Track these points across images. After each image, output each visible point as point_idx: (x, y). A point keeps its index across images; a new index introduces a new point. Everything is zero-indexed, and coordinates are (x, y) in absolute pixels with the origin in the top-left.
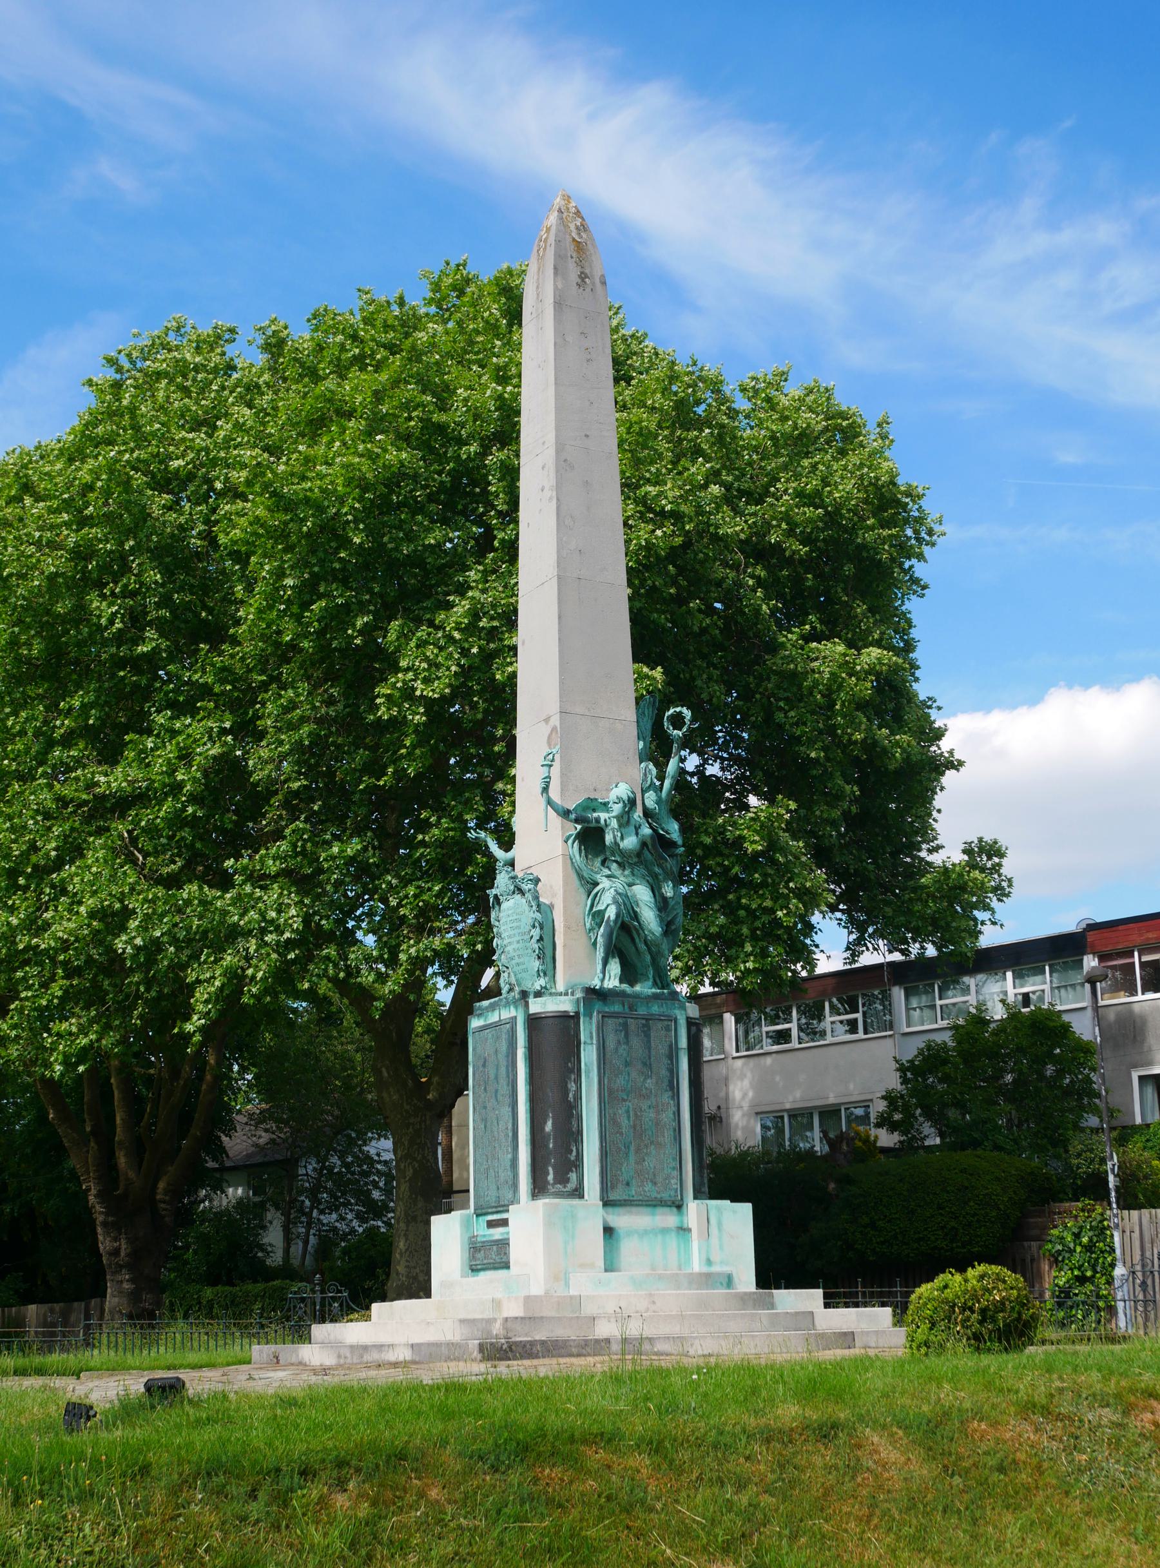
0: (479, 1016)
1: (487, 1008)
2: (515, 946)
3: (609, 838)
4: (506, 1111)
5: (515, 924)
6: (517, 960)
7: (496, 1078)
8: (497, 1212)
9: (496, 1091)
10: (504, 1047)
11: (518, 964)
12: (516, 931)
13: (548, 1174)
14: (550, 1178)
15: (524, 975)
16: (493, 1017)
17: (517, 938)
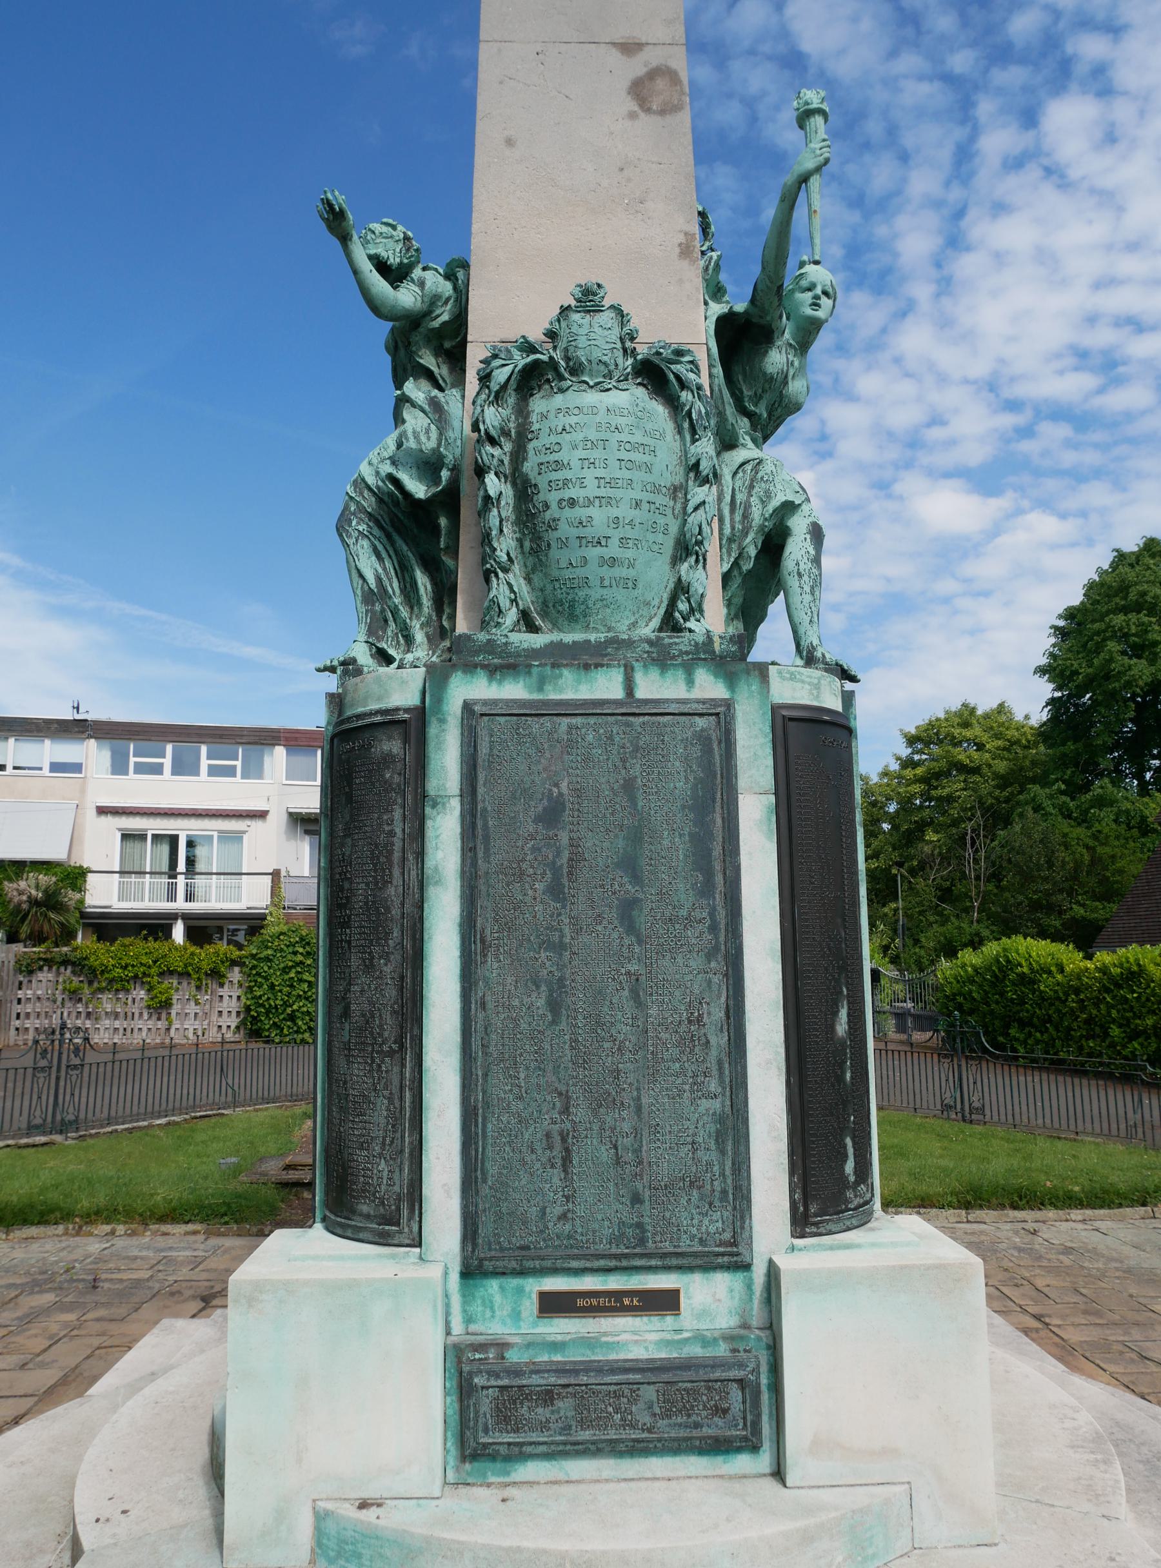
0: (493, 672)
1: (534, 653)
2: (624, 511)
3: (776, 359)
4: (689, 970)
5: (637, 457)
6: (613, 549)
7: (630, 865)
8: (608, 1270)
9: (628, 909)
10: (680, 781)
11: (613, 562)
12: (637, 476)
13: (845, 1157)
14: (849, 1167)
15: (620, 594)
16: (606, 685)
17: (637, 494)
